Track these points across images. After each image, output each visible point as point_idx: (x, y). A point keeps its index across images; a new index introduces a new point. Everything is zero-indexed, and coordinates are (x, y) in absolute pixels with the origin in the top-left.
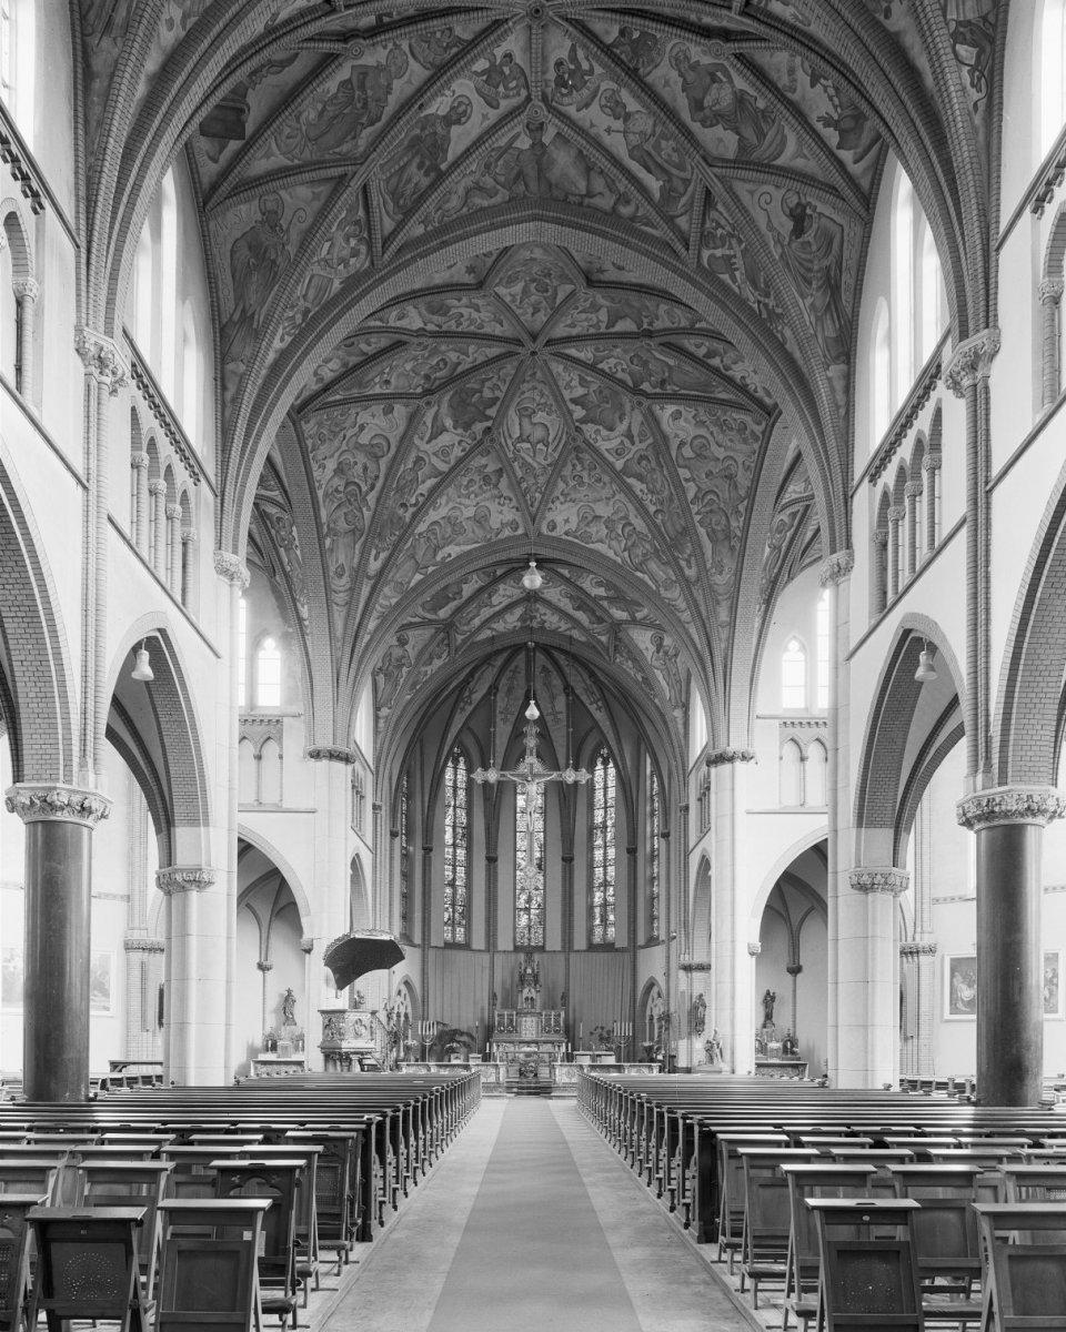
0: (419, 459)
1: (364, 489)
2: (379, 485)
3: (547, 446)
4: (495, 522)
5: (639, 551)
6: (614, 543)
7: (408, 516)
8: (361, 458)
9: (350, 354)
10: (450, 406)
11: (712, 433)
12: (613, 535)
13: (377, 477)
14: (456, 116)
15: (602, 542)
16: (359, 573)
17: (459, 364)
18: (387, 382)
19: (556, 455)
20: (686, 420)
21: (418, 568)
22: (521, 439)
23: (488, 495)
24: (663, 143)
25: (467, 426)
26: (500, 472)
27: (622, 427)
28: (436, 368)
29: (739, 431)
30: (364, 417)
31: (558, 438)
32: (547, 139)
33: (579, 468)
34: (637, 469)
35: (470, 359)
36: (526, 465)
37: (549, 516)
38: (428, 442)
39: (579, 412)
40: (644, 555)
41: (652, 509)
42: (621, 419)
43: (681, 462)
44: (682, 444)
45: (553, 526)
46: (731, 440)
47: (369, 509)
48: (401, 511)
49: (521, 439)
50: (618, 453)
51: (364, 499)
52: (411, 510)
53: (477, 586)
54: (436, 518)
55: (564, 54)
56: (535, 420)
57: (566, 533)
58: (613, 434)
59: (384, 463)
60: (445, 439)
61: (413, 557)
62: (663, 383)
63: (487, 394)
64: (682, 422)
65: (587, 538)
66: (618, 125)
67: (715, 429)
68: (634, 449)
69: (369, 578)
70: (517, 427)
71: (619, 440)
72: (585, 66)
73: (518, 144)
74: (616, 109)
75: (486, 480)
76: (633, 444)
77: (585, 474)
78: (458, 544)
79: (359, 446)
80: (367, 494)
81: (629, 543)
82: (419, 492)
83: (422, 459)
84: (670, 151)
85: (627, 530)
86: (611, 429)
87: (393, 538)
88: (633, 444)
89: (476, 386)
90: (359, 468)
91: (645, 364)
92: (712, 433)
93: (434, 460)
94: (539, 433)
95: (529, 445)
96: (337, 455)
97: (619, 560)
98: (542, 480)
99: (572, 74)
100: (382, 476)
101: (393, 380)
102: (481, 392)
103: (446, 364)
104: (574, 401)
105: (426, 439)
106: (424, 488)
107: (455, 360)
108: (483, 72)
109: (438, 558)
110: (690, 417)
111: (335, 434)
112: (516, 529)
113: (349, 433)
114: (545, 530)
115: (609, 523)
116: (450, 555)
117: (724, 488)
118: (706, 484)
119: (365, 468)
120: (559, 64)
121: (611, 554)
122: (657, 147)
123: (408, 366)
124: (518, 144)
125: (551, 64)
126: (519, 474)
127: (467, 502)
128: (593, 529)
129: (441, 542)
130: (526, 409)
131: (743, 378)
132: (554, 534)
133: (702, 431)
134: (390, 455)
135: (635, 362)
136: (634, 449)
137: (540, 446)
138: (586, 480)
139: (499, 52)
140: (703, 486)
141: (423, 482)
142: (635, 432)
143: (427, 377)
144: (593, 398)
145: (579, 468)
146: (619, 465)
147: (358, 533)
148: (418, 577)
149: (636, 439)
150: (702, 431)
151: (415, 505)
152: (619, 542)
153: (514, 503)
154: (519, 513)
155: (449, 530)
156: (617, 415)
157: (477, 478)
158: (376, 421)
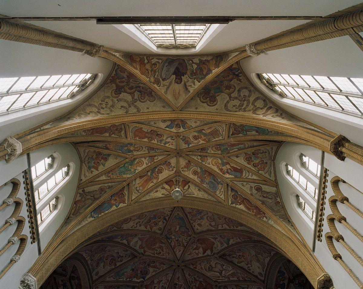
20: (202, 222)
39: (209, 252)
44: (210, 225)
49: (221, 273)
56: (214, 266)
64: (202, 224)
70: (216, 273)
77: (238, 254)
86: (214, 243)
94: (219, 266)
95: (224, 271)
104: (204, 253)
126: (235, 279)
130: (209, 268)
133: (205, 217)
137: (224, 267)
138: (241, 254)
145: (235, 256)
146: (226, 245)
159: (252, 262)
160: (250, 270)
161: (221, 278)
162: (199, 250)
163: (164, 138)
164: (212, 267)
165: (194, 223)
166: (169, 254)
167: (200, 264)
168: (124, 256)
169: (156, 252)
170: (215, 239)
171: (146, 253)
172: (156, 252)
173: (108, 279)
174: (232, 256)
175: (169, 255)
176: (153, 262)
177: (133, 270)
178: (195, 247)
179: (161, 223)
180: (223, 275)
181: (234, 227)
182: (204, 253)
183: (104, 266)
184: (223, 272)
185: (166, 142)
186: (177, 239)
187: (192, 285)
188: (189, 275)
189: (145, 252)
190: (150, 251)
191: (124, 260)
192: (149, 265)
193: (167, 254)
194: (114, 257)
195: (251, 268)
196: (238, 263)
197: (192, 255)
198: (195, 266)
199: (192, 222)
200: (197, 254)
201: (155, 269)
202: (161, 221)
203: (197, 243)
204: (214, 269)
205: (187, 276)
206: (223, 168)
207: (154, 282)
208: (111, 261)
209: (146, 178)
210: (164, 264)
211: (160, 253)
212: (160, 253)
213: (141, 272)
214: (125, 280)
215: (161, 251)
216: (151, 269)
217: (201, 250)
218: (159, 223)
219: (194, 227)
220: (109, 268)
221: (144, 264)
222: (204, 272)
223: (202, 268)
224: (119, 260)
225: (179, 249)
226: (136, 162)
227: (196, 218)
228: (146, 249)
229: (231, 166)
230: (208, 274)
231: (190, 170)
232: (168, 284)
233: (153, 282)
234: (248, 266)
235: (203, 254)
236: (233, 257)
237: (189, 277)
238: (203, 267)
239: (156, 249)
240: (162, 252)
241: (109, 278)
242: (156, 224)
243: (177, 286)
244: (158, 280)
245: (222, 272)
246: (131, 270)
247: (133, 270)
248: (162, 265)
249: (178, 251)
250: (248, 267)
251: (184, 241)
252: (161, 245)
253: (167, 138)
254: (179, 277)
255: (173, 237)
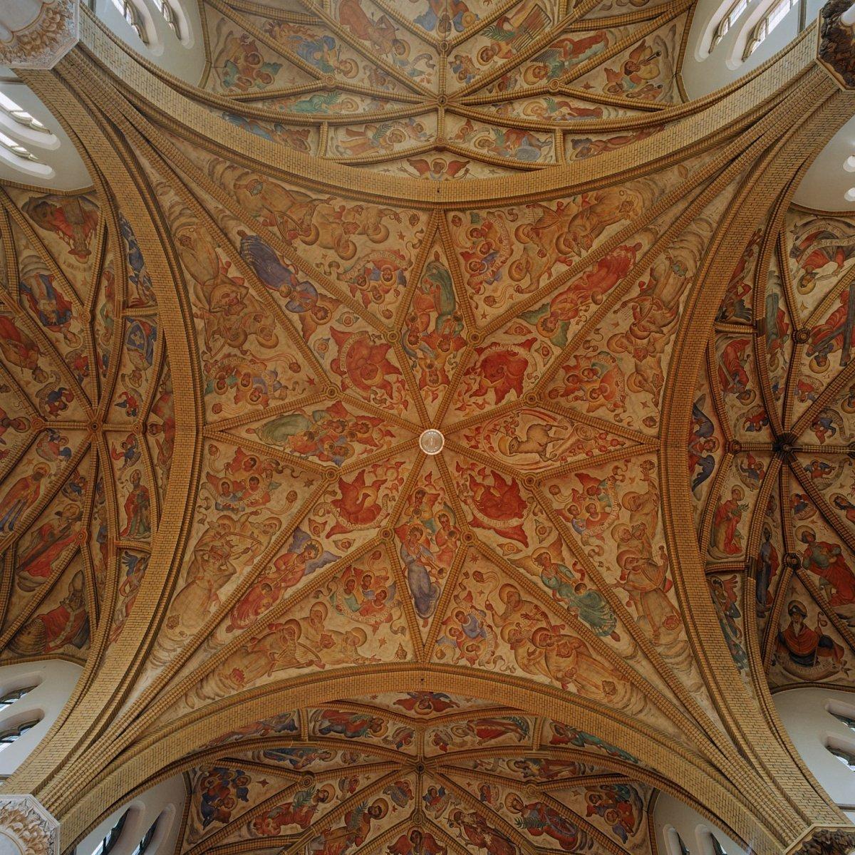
0: (540, 560)
1: (544, 625)
2: (543, 608)
3: (551, 426)
4: (641, 488)
5: (657, 314)
6: (658, 347)
7: (590, 585)
8: (516, 617)
9: (392, 598)
10: (497, 518)
11: (503, 262)
12: (651, 349)
13: (536, 607)
14: (136, 480)
15: (659, 362)
16: (622, 670)
17: (445, 504)
18: (441, 571)
19: (559, 417)
20: (495, 291)
21: (662, 592)
22: (542, 453)
23: (610, 492)
24: (138, 343)
25: (522, 505)
26: (582, 478)
27: (522, 352)
28: (445, 524)
29: (485, 236)
30: (480, 603)
31: (541, 416)
32: (161, 422)
33: (580, 393)
34: (558, 331)
35: (441, 493)
36: (572, 450)
37: (638, 425)
38: (526, 545)
39: (512, 396)
40: (659, 308)
41: (593, 308)
42: (515, 354)
43: (533, 288)
44: (519, 290)
45: (649, 421)
46: (501, 241)
47: (563, 627)
48: (583, 593)
49: (542, 453)
50: (546, 353)
51: (555, 628)
52: (586, 580)
53: (820, 523)
54: (615, 553)
55: (124, 410)
56: (525, 439)
57: (656, 405)
58: (530, 361)
59: (525, 597)
60: (529, 529)
61: (645, 593)
62: (458, 319)
63: (490, 481)
65: (658, 377)
66: (143, 373)
67: (498, 261)
68: (540, 338)
69: (632, 657)
71: (536, 354)
72: (124, 398)
73: (161, 441)
74: (136, 376)
75: (592, 492)
76: (535, 340)
77: (589, 387)
78: (654, 535)
79: (505, 617)
80: (549, 623)
81: (653, 328)
82: (571, 568)
83: (541, 554)
84: (138, 337)
85: (640, 333)
86: (526, 363)
87: (607, 610)
88: (535, 340)
89: (481, 491)
90: (524, 622)
91: (446, 338)
92: (503, 262)
93: (546, 544)
94: (538, 435)
95: (550, 445)
96: (500, 641)
97: (673, 337)
98: (592, 433)
99: (131, 407)
100: (535, 602)
101: (442, 566)
102: (489, 487)
103: (444, 515)
104: (499, 400)
105: (520, 545)
106: (569, 561)
107: (442, 507)
108: (126, 461)
109: (660, 562)
110: (491, 287)
111: (482, 634)
112: (651, 463)
113: (490, 622)
114: (653, 431)
115: (640, 355)
116: (661, 548)
117: (551, 232)
118: (552, 254)
119: (526, 616)
120: (128, 414)
121: (669, 349)
122: (141, 346)
123: (435, 548)
124: (161, 441)
125: (127, 418)
126: (582, 456)
127: (612, 517)
128: (650, 374)
129: (646, 555)
130: (511, 446)
131: (414, 246)
132: (658, 420)
133: (504, 271)
134: (518, 587)
135: (447, 347)
136: (540, 338)
137: (551, 434)
138: (597, 385)
139: (119, 450)
140: (554, 256)
141: (563, 560)
142: (522, 339)
143: (451, 534)
144: (499, 383)
145: (580, 393)
146: (557, 351)
147: (582, 649)
148: (671, 593)
149: (529, 337)
150: (504, 271)
151: (583, 575)
152: (655, 340)
153: (620, 464)
154: (633, 460)
155: (636, 542)
156: (511, 359)
157: (588, 502)
158: (487, 592)
159: (628, 398)
160: (621, 421)
161: (543, 464)
162: (486, 396)
163: (411, 59)
164: (520, 443)
165: (476, 297)
166: (406, 404)
167: (488, 438)
168: (290, 387)
169: (372, 396)
170: (528, 344)
171: (348, 391)
172: (372, 396)
173: (244, 434)
174: (573, 395)
175: (406, 408)
176: (365, 429)
177: (311, 435)
178: (475, 387)
179: (390, 297)
180: (548, 456)
181: (580, 256)
182: (499, 400)
183: (237, 400)
184: (550, 448)
185: (414, 70)
186: (428, 361)
187: (465, 494)
188: (458, 468)
189: (344, 387)
190: (358, 390)
191: (289, 397)
192: (352, 435)
193: (401, 406)
194: (264, 384)
195: (623, 416)
196: (588, 411)
197: (467, 411)
198: (473, 443)
199: (470, 291)
200: (481, 407)
201: (369, 447)
202: (392, 291)
203: (479, 375)
204: (523, 447)
205: (452, 469)
206: (553, 114)
207: (364, 483)
208: (257, 394)
209: (363, 141)
210: (392, 436)
211: (383, 401)
212: (383, 401)
213: (331, 447)
214: (288, 451)
215: (385, 396)
216: (358, 447)
217: (491, 396)
218: (387, 296)
219: (474, 310)
220: (249, 407)
221: (340, 429)
222: (499, 456)
223: (491, 448)
224: (277, 394)
225: (433, 392)
226: (339, 101)
227: (481, 278)
228: (347, 381)
229: (571, 109)
230: (510, 461)
231: (469, 141)
232: (400, 488)
233: (360, 479)
234: (616, 412)
235: (496, 403)
236: (576, 398)
237: (457, 474)
238: (495, 445)
239: (374, 388)
240: (389, 400)
241: (248, 431)
242: (379, 298)
243: (424, 500)
244: (375, 479)
245: (545, 449)
246: (305, 435)
247: (311, 435)
248: (388, 438)
249: (430, 398)
250: (617, 415)
251: (447, 367)
252: (387, 377)
253: (418, 59)
254: (430, 475)
255: (420, 354)
